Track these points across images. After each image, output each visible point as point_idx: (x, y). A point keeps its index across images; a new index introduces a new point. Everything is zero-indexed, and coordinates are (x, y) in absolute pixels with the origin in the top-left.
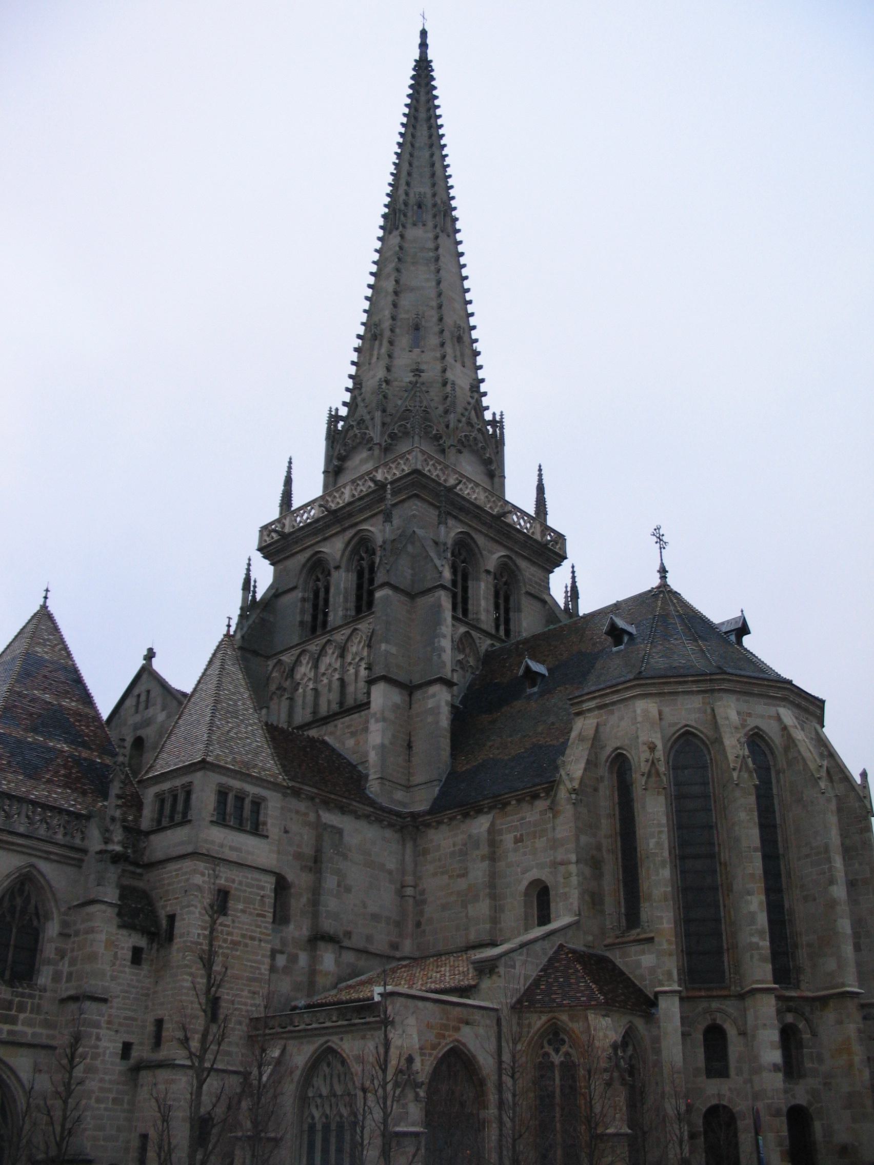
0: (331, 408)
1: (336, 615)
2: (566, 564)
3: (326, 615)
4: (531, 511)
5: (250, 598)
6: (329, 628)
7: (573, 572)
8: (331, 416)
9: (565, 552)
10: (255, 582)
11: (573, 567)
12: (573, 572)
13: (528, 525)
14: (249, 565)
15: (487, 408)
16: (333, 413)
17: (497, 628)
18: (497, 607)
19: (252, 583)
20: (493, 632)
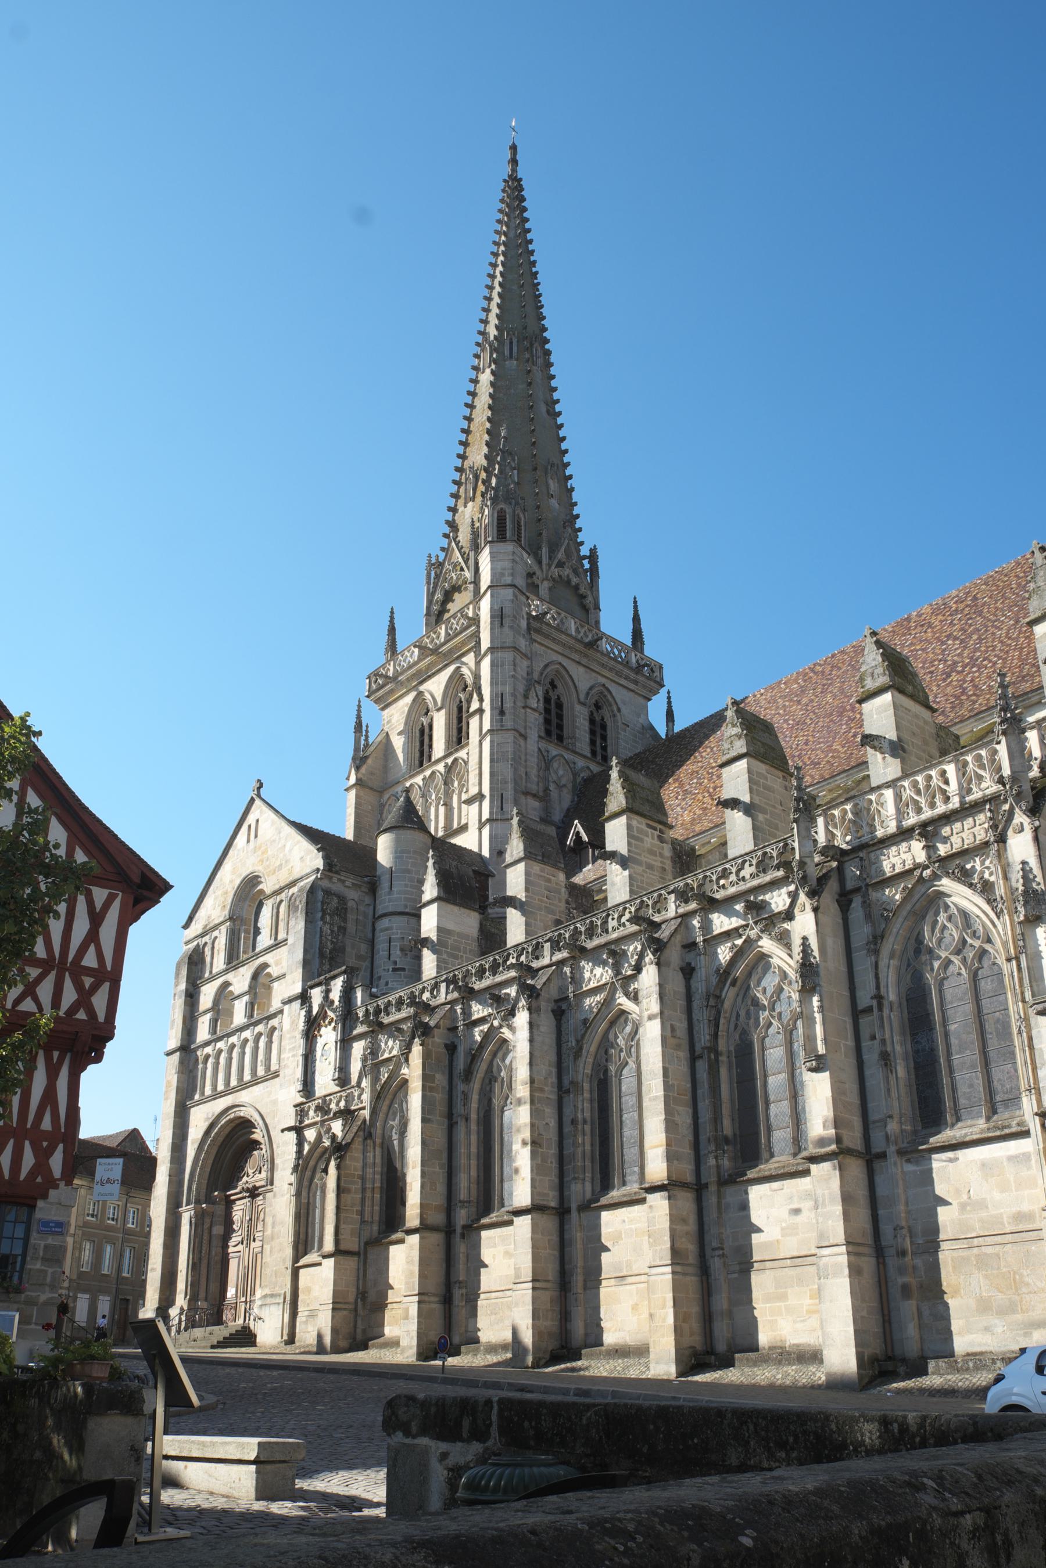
0: (430, 556)
1: (439, 747)
2: (663, 692)
3: (431, 746)
4: (628, 641)
5: (363, 742)
6: (433, 760)
7: (669, 698)
8: (431, 565)
9: (662, 679)
10: (367, 726)
11: (669, 692)
12: (669, 698)
13: (623, 655)
14: (359, 711)
15: (582, 543)
16: (433, 560)
17: (594, 753)
18: (592, 732)
19: (364, 728)
20: (589, 755)
